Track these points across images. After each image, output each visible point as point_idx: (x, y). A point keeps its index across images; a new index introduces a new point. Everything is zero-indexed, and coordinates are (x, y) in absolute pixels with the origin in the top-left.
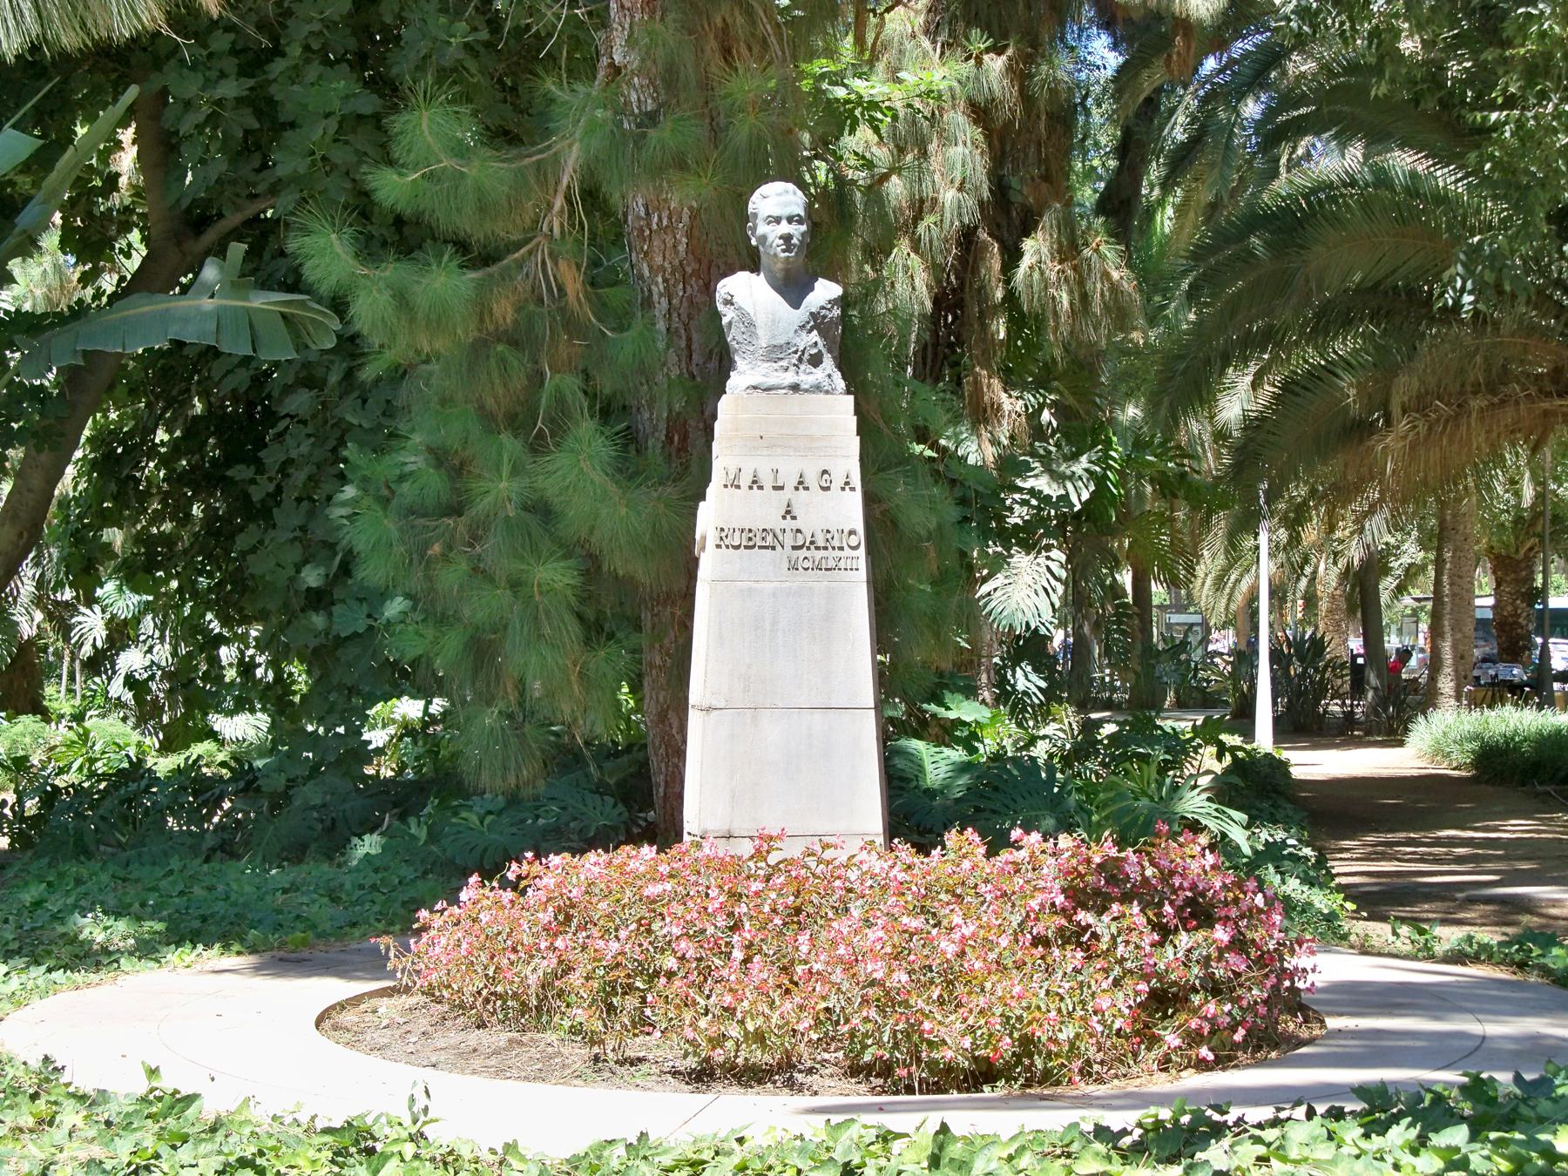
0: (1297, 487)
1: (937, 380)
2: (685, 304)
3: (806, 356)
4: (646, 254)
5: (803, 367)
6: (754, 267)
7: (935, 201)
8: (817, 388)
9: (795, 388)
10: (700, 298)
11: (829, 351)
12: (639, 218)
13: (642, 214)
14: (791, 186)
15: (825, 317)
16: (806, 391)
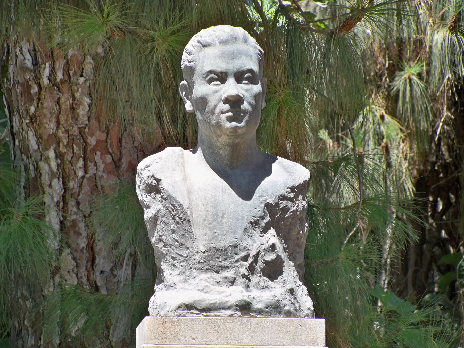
0: (304, 206)
1: (421, 292)
2: (86, 188)
3: (260, 265)
4: (33, 119)
5: (255, 279)
6: (188, 142)
7: (420, 43)
8: (275, 308)
9: (245, 308)
10: (108, 181)
11: (292, 257)
12: (24, 69)
13: (29, 63)
14: (240, 31)
15: (285, 210)
16: (260, 312)
